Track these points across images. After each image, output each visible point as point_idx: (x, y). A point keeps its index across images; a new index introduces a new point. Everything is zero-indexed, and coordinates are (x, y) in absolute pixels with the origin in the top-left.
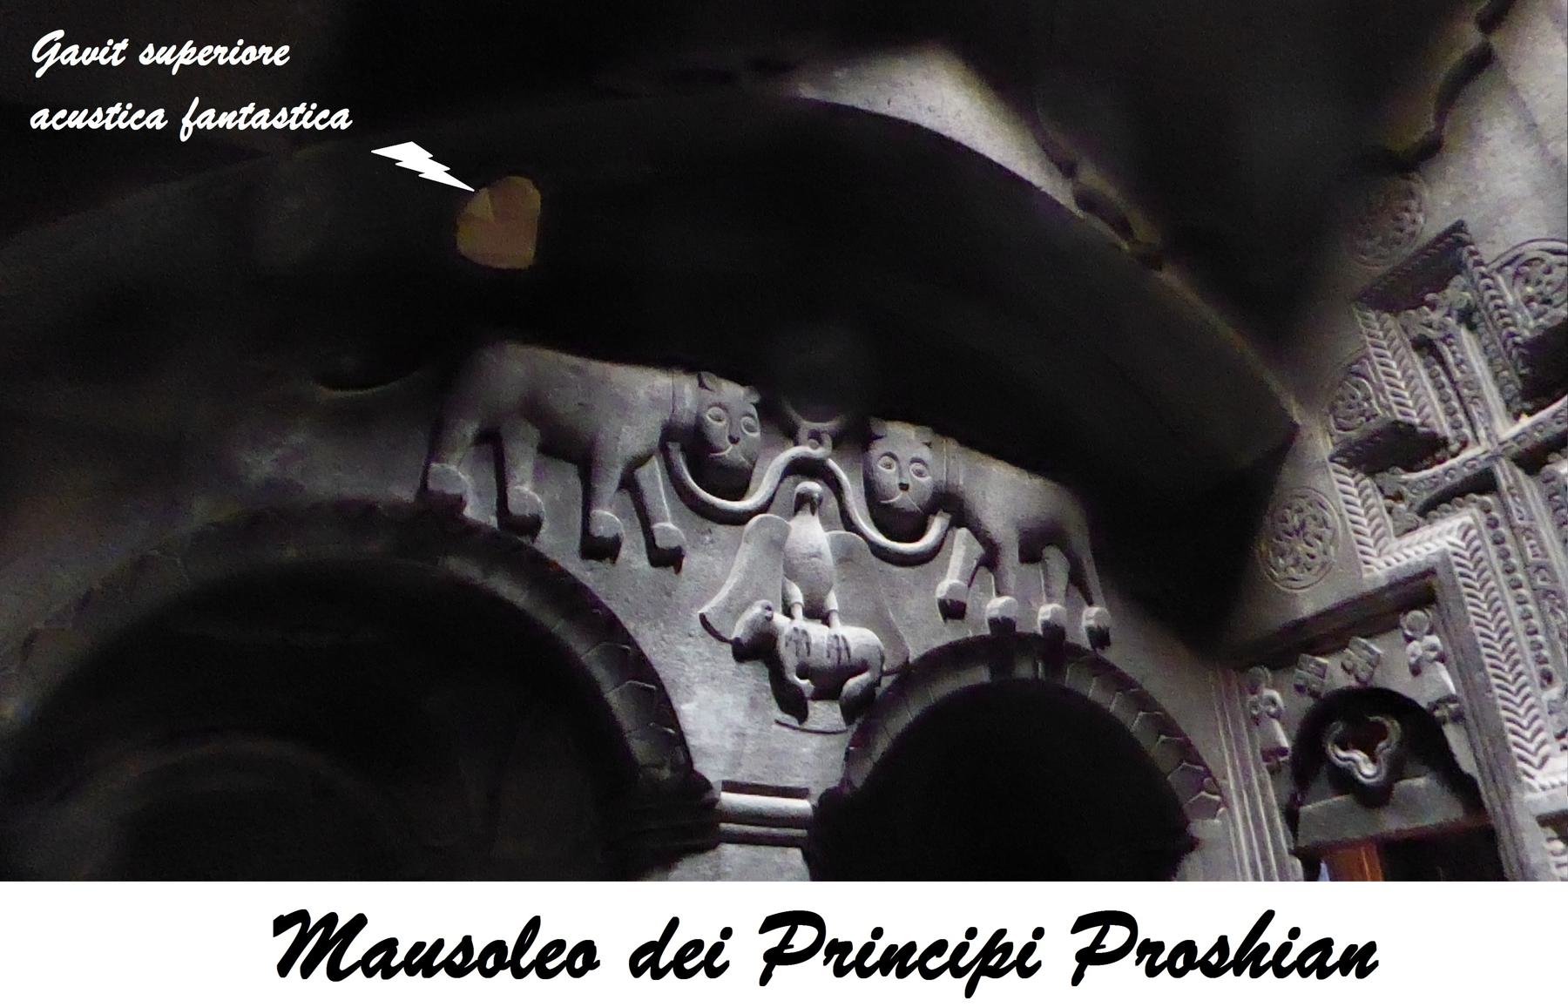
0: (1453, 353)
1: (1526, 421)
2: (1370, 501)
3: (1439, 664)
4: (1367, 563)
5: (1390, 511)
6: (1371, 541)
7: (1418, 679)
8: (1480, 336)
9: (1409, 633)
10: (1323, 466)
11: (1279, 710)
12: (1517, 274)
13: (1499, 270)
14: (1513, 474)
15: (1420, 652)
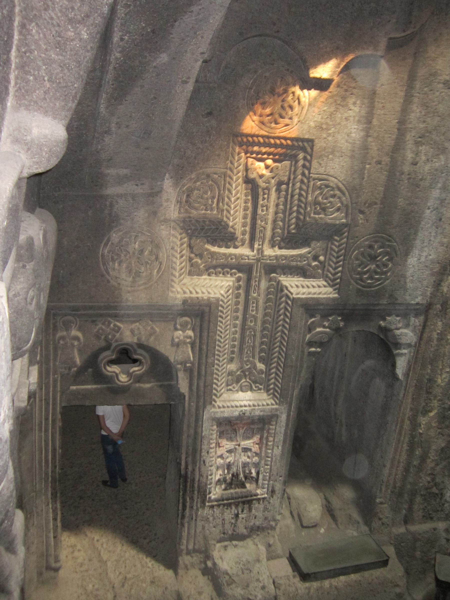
0: (264, 199)
1: (279, 252)
2: (184, 252)
3: (189, 346)
4: (173, 287)
5: (191, 259)
6: (177, 274)
7: (174, 349)
8: (279, 198)
9: (179, 327)
10: (166, 221)
11: (80, 344)
12: (320, 188)
13: (314, 179)
14: (260, 272)
15: (182, 338)
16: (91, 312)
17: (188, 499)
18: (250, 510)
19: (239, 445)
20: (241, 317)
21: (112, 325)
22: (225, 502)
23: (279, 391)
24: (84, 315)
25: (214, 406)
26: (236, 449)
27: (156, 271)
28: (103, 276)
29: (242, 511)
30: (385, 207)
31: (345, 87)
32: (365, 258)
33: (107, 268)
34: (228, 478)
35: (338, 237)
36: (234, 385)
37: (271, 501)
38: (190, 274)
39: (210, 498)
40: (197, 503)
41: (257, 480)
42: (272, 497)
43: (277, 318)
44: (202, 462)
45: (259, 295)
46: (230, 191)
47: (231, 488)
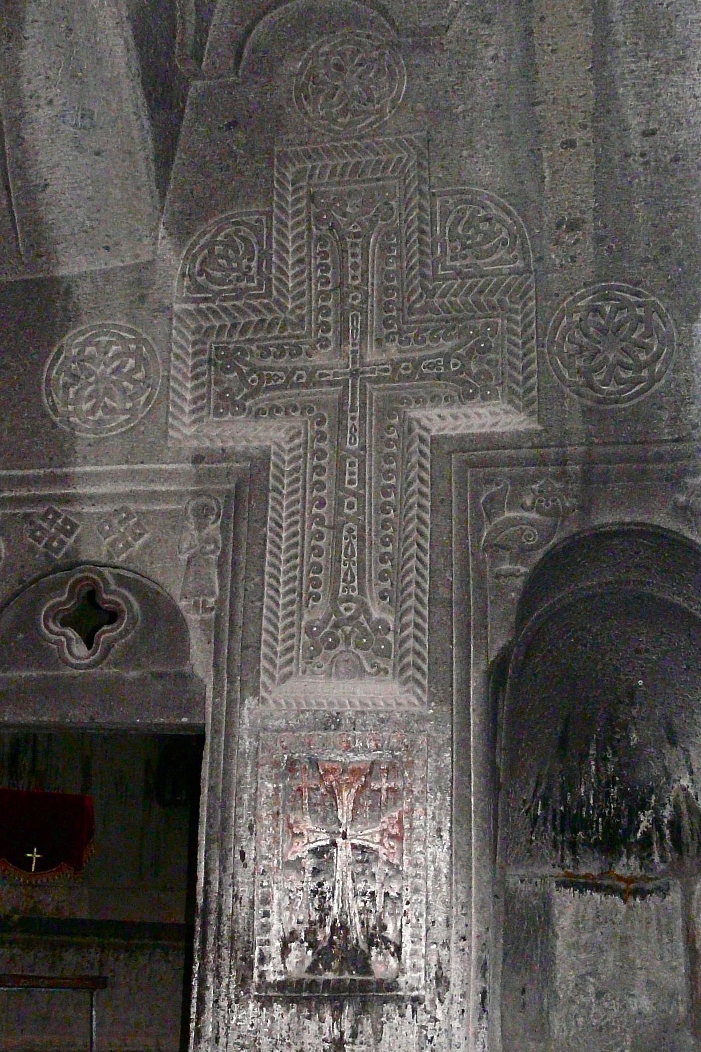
16: (23, 492)
17: (210, 979)
18: (378, 1035)
19: (344, 836)
20: (330, 502)
21: (60, 521)
22: (304, 995)
23: (425, 667)
24: (11, 499)
25: (264, 701)
26: (334, 844)
27: (143, 399)
28: (45, 415)
29: (354, 1035)
30: (605, 226)
31: (471, 38)
32: (586, 336)
33: (53, 401)
34: (320, 937)
35: (518, 304)
36: (322, 662)
37: (439, 1016)
38: (217, 414)
39: (262, 975)
40: (228, 985)
41: (398, 949)
42: (442, 1002)
43: (406, 491)
44: (238, 856)
45: (363, 448)
46: (282, 245)
47: (327, 967)
